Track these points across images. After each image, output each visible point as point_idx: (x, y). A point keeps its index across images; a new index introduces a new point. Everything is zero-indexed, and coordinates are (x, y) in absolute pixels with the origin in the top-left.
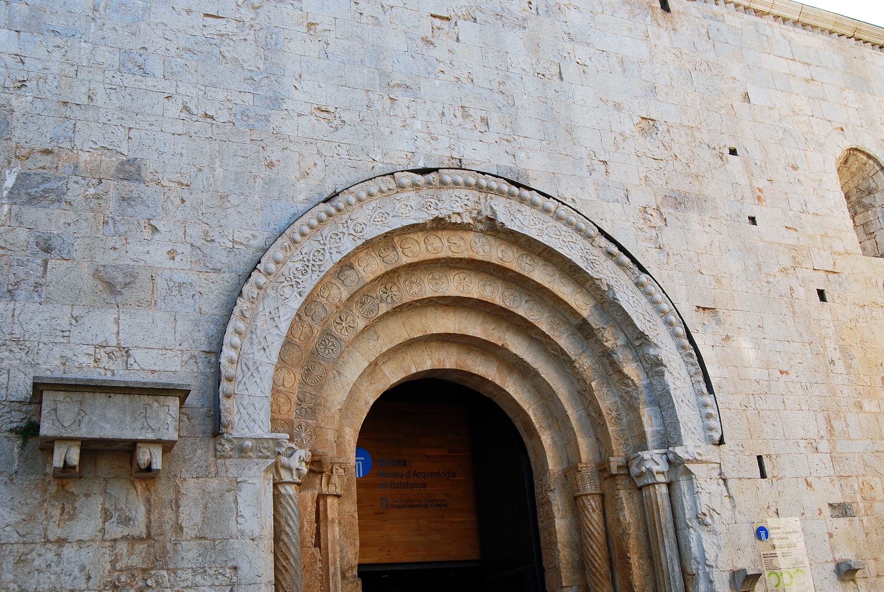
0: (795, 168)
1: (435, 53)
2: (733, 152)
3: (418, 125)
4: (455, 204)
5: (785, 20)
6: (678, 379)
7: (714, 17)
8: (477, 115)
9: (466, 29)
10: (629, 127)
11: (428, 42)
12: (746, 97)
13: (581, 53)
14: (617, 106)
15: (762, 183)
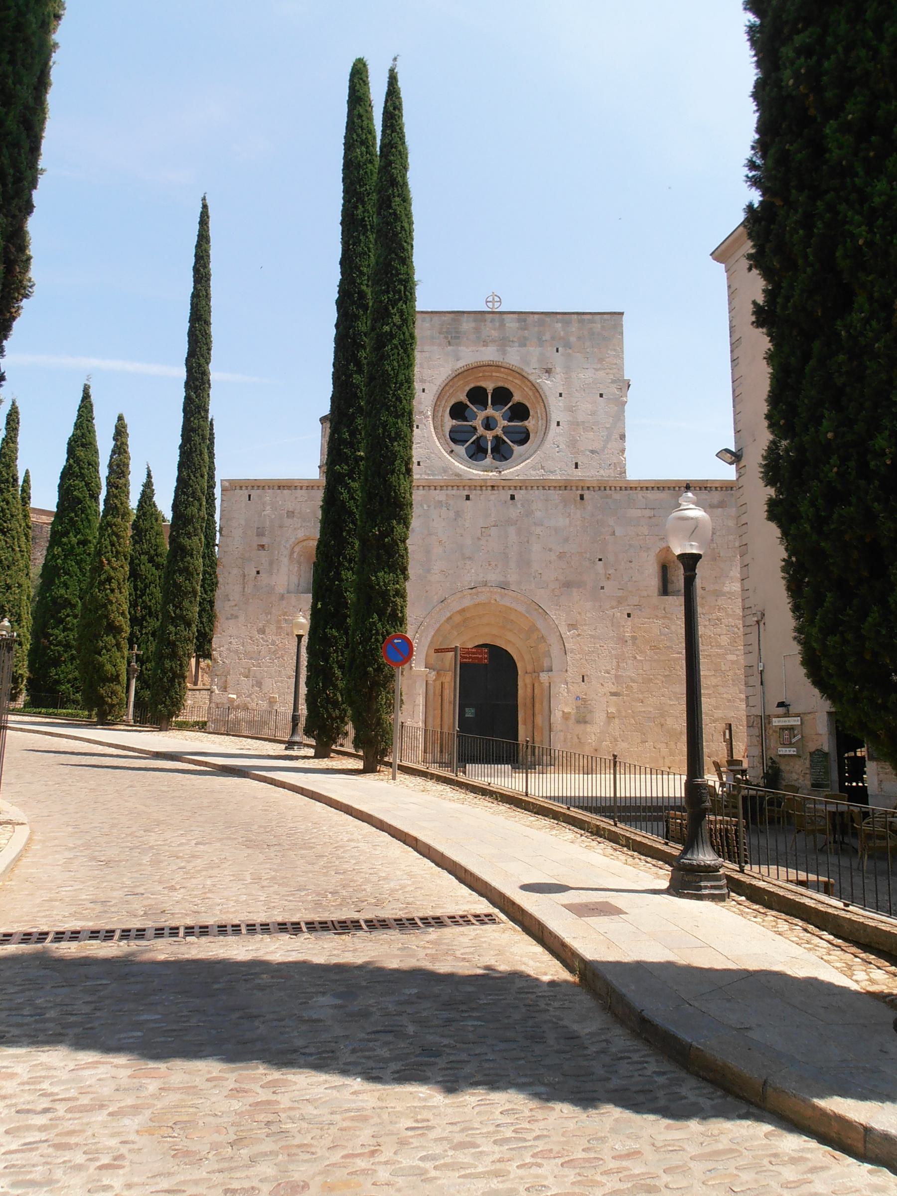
0: (631, 562)
1: (481, 542)
2: (600, 560)
3: (473, 571)
4: (483, 598)
5: (647, 488)
6: (555, 650)
7: (607, 497)
8: (493, 564)
9: (494, 531)
10: (553, 557)
11: (479, 539)
12: (613, 533)
13: (538, 530)
14: (550, 550)
15: (611, 571)
